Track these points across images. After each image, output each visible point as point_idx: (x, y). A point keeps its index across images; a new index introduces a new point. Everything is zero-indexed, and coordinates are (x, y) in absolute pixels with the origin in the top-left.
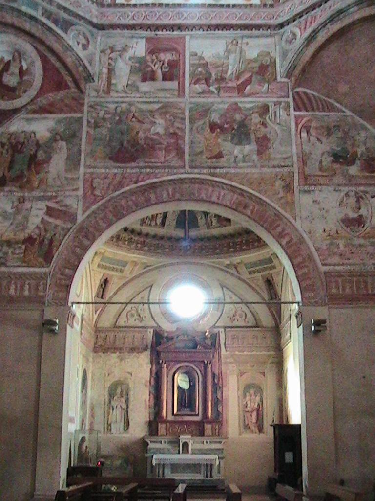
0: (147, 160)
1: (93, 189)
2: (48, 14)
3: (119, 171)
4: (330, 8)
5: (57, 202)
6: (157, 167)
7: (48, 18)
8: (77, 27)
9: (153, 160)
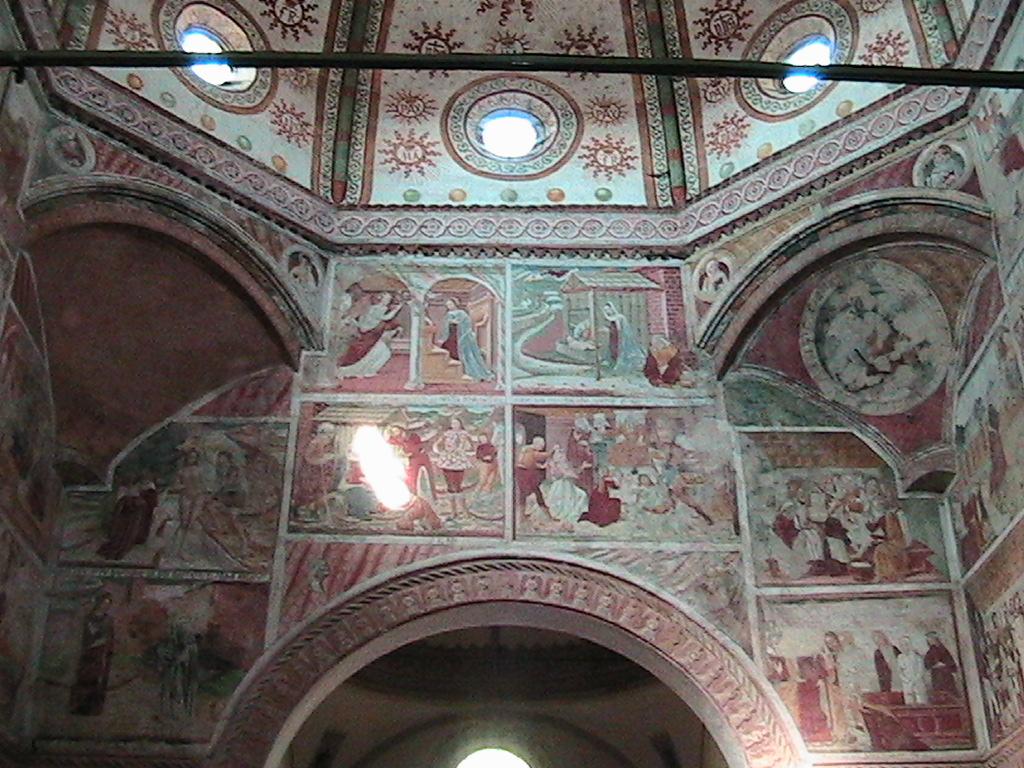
4: (170, 182)
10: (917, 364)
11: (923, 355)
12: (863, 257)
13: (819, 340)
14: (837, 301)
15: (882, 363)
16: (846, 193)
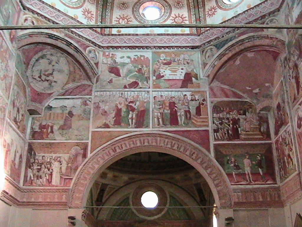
10: (50, 84)
11: (53, 84)
12: (62, 54)
13: (37, 60)
14: (48, 56)
15: (43, 77)
16: (71, 38)
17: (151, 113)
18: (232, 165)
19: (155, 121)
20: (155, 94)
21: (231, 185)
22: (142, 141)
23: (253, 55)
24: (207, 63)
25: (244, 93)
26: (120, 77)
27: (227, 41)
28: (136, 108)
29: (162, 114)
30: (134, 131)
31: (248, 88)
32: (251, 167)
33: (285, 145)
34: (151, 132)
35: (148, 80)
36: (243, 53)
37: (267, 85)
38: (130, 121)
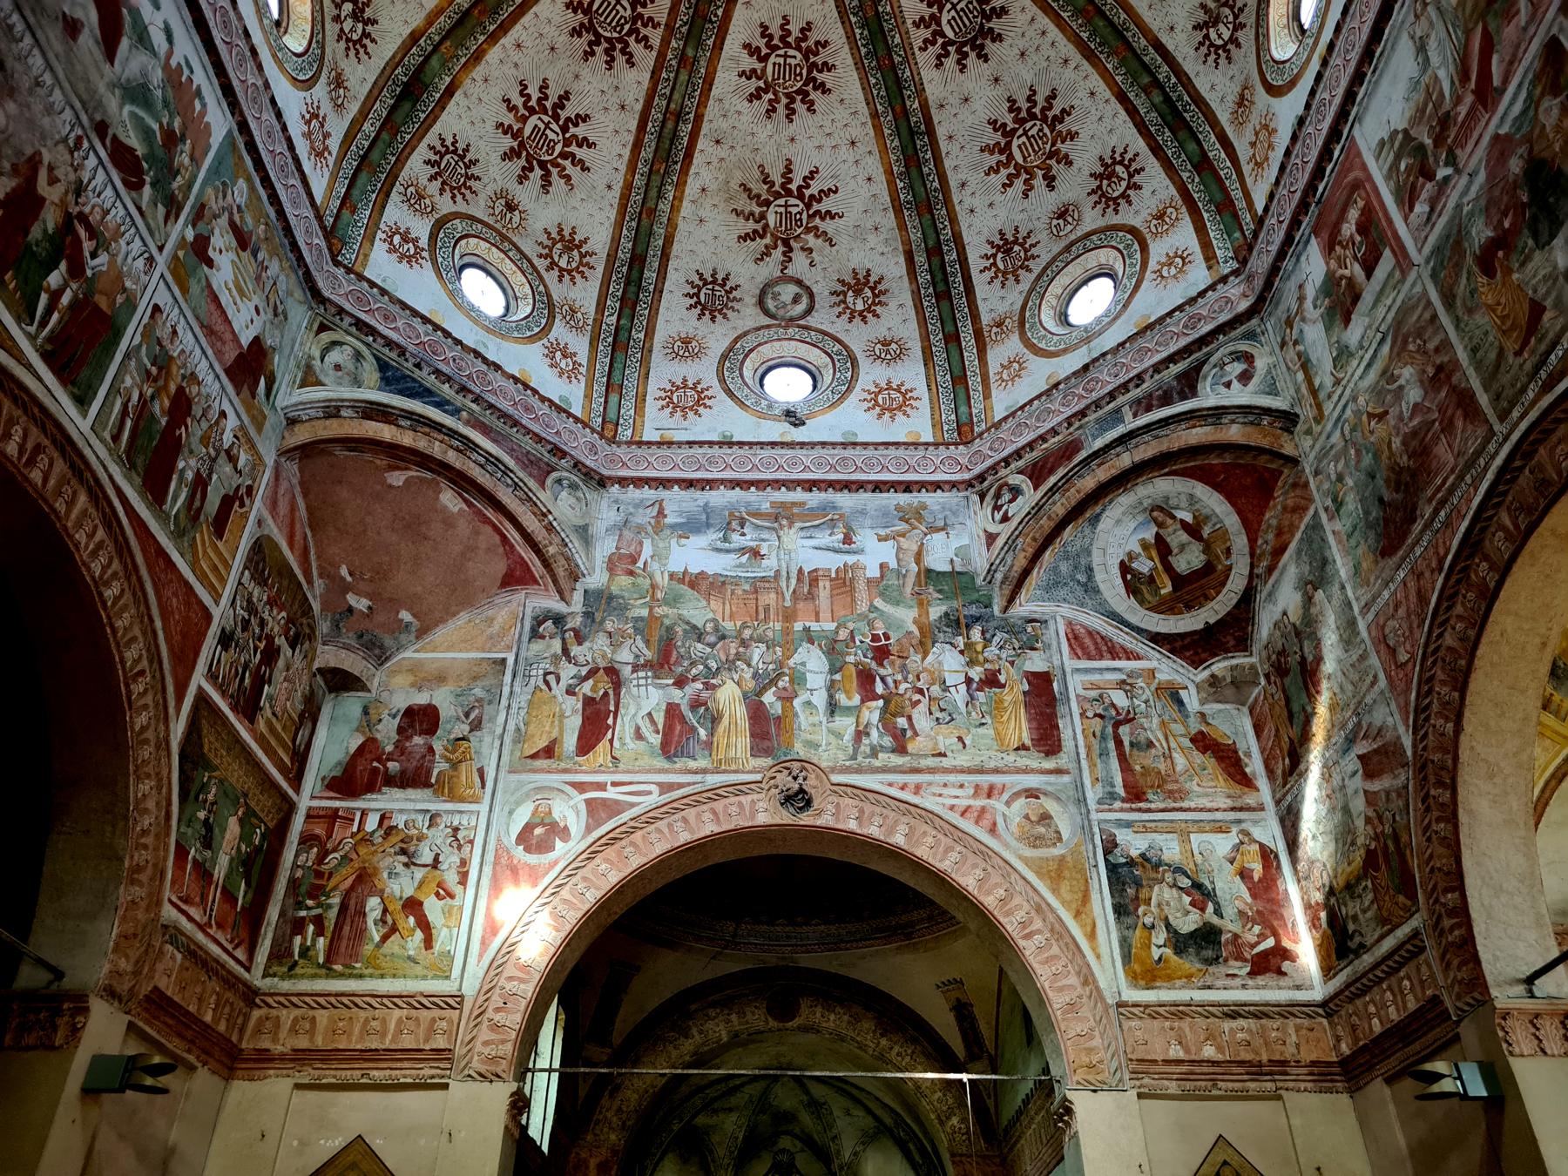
0: (1429, 493)
1: (1393, 651)
2: (1144, 404)
3: (1406, 567)
5: (1365, 737)
6: (1451, 492)
7: (1149, 409)
8: (1213, 360)
9: (1439, 481)
17: (118, 357)
18: (202, 815)
19: (113, 404)
20: (163, 298)
21: (170, 901)
22: (29, 446)
23: (456, 510)
24: (323, 378)
25: (321, 576)
26: (108, 65)
27: (423, 393)
28: (89, 273)
29: (144, 402)
30: (29, 367)
31: (344, 571)
32: (232, 859)
33: (404, 859)
34: (81, 443)
35: (172, 218)
36: (439, 474)
37: (405, 616)
38: (44, 299)
